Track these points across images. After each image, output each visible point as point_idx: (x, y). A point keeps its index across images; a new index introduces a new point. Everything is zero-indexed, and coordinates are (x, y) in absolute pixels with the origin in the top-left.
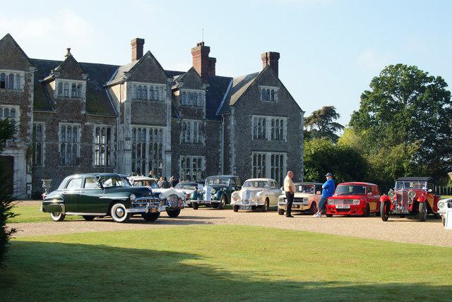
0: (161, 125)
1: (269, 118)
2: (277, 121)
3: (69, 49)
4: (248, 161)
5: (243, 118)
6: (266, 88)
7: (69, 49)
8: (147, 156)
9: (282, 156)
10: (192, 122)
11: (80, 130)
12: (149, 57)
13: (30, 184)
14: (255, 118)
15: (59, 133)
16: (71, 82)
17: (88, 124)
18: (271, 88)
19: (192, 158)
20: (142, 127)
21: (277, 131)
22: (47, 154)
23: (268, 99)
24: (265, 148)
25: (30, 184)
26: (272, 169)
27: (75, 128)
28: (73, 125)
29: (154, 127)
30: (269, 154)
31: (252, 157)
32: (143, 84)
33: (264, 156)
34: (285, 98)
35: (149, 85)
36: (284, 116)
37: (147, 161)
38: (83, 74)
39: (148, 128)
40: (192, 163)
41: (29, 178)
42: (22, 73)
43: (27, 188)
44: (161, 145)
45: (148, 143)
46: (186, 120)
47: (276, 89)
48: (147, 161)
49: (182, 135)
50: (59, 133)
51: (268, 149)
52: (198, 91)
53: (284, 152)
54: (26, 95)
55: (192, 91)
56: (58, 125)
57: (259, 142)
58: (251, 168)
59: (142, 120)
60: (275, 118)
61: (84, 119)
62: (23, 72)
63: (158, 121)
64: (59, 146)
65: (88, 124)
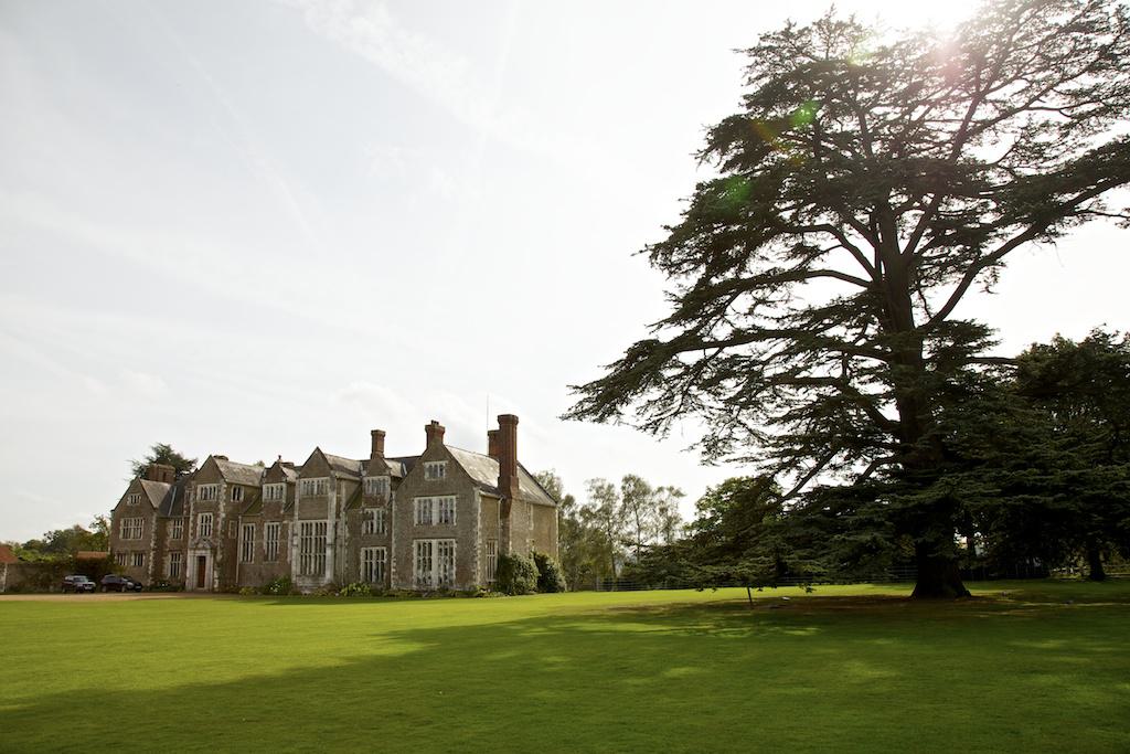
0: (322, 518)
1: (435, 499)
2: (446, 500)
5: (404, 502)
6: (433, 464)
8: (313, 551)
10: (375, 511)
14: (420, 502)
15: (265, 533)
16: (274, 485)
17: (285, 522)
18: (438, 463)
19: (374, 549)
20: (309, 522)
21: (446, 513)
23: (435, 476)
28: (275, 524)
29: (319, 521)
31: (415, 546)
32: (310, 480)
35: (315, 480)
36: (453, 494)
37: (313, 555)
39: (313, 522)
40: (374, 555)
41: (216, 576)
42: (215, 485)
43: (214, 583)
45: (313, 538)
46: (369, 510)
47: (444, 463)
48: (313, 555)
49: (364, 525)
50: (265, 533)
51: (434, 535)
52: (381, 478)
55: (375, 478)
59: (308, 515)
60: (443, 498)
61: (283, 518)
63: (322, 515)
64: (265, 544)
65: (285, 522)
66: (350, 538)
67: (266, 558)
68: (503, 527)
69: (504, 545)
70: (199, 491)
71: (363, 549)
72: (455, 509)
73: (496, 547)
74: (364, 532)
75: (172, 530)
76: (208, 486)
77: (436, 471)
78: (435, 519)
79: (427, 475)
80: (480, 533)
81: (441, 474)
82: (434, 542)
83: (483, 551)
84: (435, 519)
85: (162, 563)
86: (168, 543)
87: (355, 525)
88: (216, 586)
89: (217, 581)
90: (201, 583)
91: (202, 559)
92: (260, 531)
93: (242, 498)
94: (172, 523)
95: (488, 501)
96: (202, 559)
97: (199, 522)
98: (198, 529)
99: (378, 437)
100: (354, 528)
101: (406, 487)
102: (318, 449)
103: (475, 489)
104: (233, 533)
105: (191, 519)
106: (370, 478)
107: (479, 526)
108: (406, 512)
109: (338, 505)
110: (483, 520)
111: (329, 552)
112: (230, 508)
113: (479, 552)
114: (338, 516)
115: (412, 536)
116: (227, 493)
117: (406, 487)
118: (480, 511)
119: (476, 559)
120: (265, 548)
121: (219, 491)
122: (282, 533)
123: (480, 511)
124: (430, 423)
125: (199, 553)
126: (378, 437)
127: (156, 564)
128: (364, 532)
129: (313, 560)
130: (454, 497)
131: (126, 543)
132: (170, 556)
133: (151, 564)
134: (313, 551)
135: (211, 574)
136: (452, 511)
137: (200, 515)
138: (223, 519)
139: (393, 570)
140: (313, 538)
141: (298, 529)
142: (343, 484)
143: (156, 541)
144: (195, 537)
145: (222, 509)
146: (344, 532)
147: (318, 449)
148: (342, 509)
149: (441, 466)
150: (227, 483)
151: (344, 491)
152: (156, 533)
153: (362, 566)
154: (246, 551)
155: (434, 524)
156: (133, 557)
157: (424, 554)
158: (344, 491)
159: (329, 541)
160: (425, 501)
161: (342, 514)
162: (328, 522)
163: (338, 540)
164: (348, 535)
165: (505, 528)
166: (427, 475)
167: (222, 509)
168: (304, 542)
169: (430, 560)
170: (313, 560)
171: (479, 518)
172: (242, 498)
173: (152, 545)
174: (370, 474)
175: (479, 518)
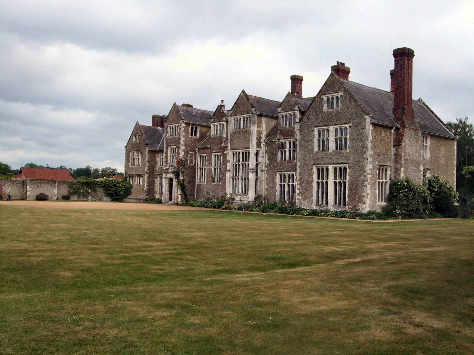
1: (332, 128)
3: (222, 101)
4: (310, 175)
5: (307, 132)
6: (330, 96)
7: (222, 101)
9: (345, 169)
11: (222, 157)
12: (242, 94)
13: (179, 195)
14: (319, 131)
16: (218, 124)
18: (335, 95)
19: (287, 174)
22: (207, 175)
23: (332, 107)
24: (326, 161)
25: (179, 195)
26: (335, 183)
27: (220, 156)
30: (331, 168)
31: (315, 170)
33: (327, 169)
34: (348, 102)
38: (223, 117)
43: (178, 198)
44: (248, 164)
49: (279, 154)
50: (213, 160)
51: (330, 161)
53: (348, 163)
54: (179, 139)
56: (211, 155)
57: (321, 155)
58: (312, 182)
59: (237, 146)
60: (338, 127)
62: (178, 124)
63: (246, 145)
64: (213, 169)
65: (225, 152)
66: (269, 165)
67: (213, 180)
68: (396, 155)
69: (397, 171)
70: (169, 129)
71: (278, 174)
72: (348, 137)
73: (388, 172)
74: (279, 159)
75: (159, 160)
76: (173, 126)
77: (333, 103)
78: (332, 146)
79: (325, 107)
80: (370, 159)
81: (337, 106)
82: (331, 168)
83: (373, 176)
84: (332, 146)
85: (154, 183)
86: (157, 169)
87: (273, 154)
88: (179, 200)
89: (180, 196)
90: (171, 199)
91: (171, 180)
92: (210, 159)
93: (198, 135)
94: (159, 154)
95: (380, 129)
96: (171, 180)
97: (169, 153)
98: (169, 158)
99: (296, 81)
100: (272, 157)
101: (308, 118)
102: (243, 92)
103: (366, 117)
104: (191, 161)
105: (165, 151)
106: (284, 114)
107: (370, 152)
108: (307, 140)
109: (259, 138)
110: (374, 147)
111: (252, 176)
112: (189, 143)
113: (369, 176)
114: (259, 146)
115: (312, 162)
116: (186, 132)
117: (308, 118)
118: (370, 138)
119: (366, 183)
120: (213, 172)
121: (180, 129)
122: (223, 160)
123: (370, 138)
124: (336, 64)
125: (171, 175)
126: (296, 81)
127: (149, 183)
128: (279, 159)
129: (240, 181)
130: (348, 126)
131: (132, 169)
132: (159, 178)
133: (146, 183)
134: (241, 174)
135: (177, 192)
136: (346, 139)
137: (169, 148)
138: (184, 150)
139: (297, 191)
140: (240, 163)
141: (230, 157)
142: (263, 120)
143: (149, 167)
144: (167, 164)
145: (182, 143)
146: (264, 159)
147: (243, 92)
148: (262, 140)
149: (337, 97)
150: (185, 123)
151: (264, 125)
152: (149, 161)
153: (278, 188)
154: (201, 175)
155: (330, 151)
156: (136, 179)
157: (323, 178)
158: (264, 125)
159: (251, 167)
160: (323, 130)
161: (263, 145)
162: (250, 151)
163: (259, 166)
164: (267, 162)
165: (397, 155)
166: (325, 107)
167: (182, 143)
168: (235, 166)
169: (327, 183)
170: (240, 181)
171: (370, 145)
172: (198, 135)
173: (146, 170)
174: (284, 110)
175: (370, 145)
